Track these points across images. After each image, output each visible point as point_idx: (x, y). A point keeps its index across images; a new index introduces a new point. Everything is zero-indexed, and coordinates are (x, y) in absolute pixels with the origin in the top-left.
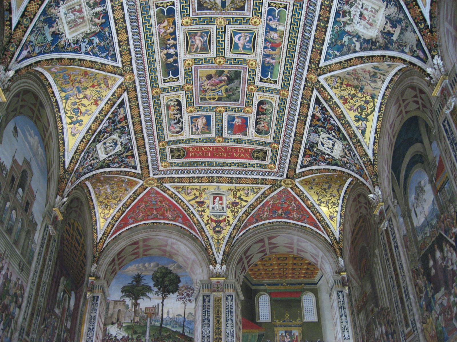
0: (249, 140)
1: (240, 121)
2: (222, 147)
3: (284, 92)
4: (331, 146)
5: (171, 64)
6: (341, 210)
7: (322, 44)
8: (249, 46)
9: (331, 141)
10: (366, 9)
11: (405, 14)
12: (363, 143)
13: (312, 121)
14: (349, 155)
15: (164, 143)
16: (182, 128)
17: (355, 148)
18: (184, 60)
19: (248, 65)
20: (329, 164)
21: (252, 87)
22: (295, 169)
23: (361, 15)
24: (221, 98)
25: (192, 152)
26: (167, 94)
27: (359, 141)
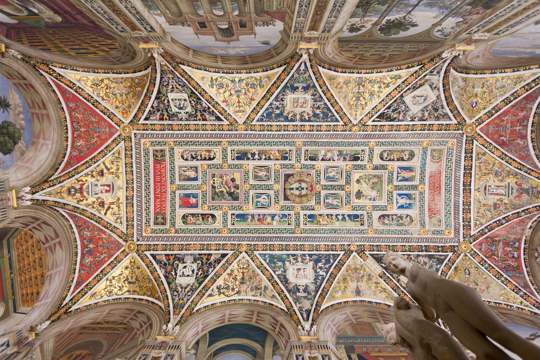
4: (186, 274)
6: (105, 301)
7: (271, 250)
9: (191, 273)
10: (304, 271)
11: (316, 295)
12: (203, 299)
13: (205, 254)
14: (186, 290)
17: (198, 294)
20: (166, 277)
22: (149, 250)
23: (299, 269)
27: (204, 295)
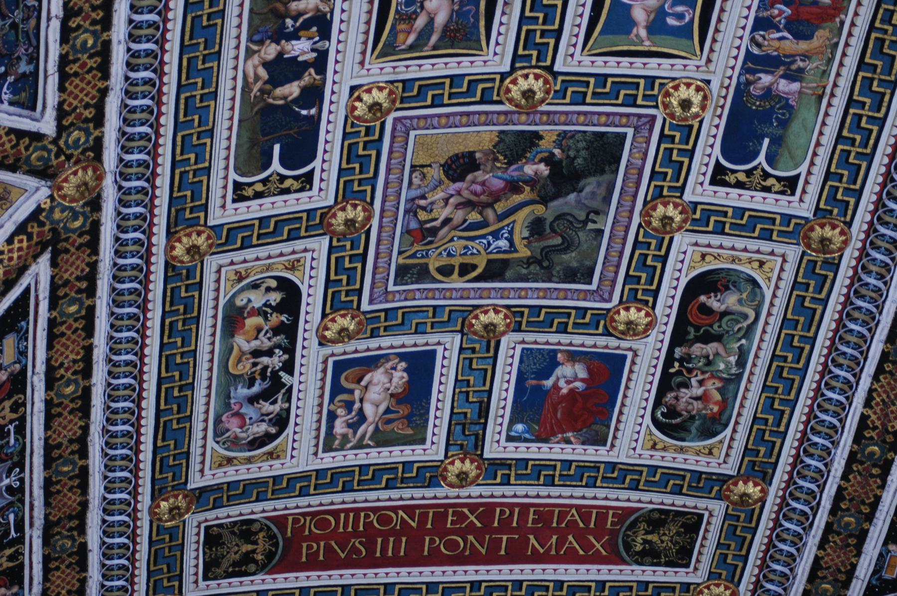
0: (613, 466)
1: (583, 374)
2: (473, 508)
3: (828, 232)
5: (287, 108)
8: (680, 16)
15: (181, 502)
16: (281, 421)
18: (353, 89)
19: (666, 106)
21: (671, 211)
24: (505, 263)
25: (313, 537)
26: (238, 256)
